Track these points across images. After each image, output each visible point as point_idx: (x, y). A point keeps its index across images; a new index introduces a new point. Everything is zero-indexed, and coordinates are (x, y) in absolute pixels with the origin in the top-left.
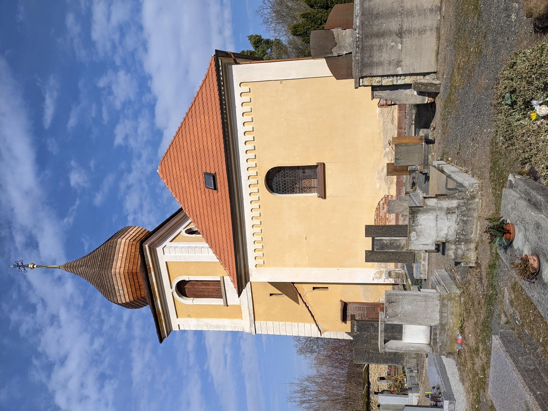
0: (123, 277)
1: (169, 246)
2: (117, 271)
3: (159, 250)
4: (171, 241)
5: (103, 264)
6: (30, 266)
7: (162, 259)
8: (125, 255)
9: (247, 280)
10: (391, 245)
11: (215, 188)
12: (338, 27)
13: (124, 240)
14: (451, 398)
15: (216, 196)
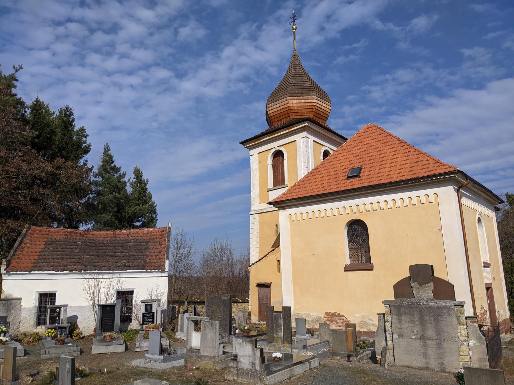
0: (286, 106)
1: (309, 141)
2: (290, 101)
3: (305, 134)
4: (314, 141)
5: (295, 88)
6: (294, 26)
8: (303, 105)
9: (280, 208)
10: (278, 326)
11: (348, 178)
12: (435, 287)
13: (315, 101)
14: (165, 361)
15: (343, 178)
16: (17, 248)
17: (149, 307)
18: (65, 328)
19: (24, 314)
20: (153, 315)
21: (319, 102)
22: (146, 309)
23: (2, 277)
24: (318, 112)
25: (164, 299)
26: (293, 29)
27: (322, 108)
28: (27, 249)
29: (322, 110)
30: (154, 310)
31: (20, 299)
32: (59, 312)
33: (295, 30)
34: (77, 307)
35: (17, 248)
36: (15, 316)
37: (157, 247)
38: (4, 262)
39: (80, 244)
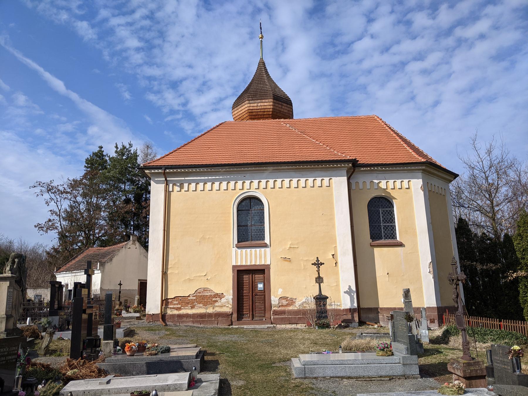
21: (252, 105)
23: (55, 276)
24: (254, 114)
26: (260, 38)
27: (258, 108)
29: (259, 110)
33: (262, 38)
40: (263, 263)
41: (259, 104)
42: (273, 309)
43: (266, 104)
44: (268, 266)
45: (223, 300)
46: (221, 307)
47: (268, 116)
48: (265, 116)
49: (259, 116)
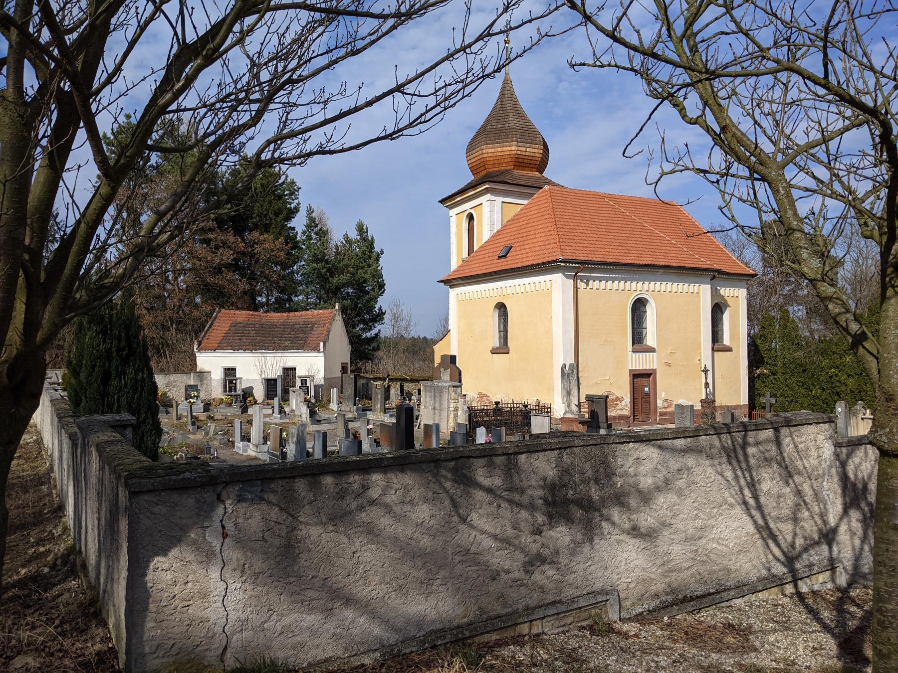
0: (481, 157)
2: (484, 151)
3: (488, 196)
7: (483, 199)
8: (500, 154)
9: (452, 287)
10: (378, 399)
11: (500, 257)
13: (513, 148)
14: (281, 418)
16: (208, 330)
17: (304, 382)
18: (239, 395)
19: (214, 384)
20: (308, 389)
21: (521, 149)
22: (302, 384)
24: (520, 160)
25: (321, 375)
27: (527, 154)
28: (215, 331)
30: (308, 384)
31: (210, 372)
32: (236, 383)
34: (252, 380)
35: (208, 330)
36: (207, 385)
37: (321, 329)
38: (196, 343)
39: (257, 326)
40: (651, 368)
41: (528, 150)
42: (659, 410)
43: (535, 151)
44: (655, 370)
45: (623, 403)
46: (621, 410)
47: (534, 166)
48: (530, 166)
49: (525, 165)
